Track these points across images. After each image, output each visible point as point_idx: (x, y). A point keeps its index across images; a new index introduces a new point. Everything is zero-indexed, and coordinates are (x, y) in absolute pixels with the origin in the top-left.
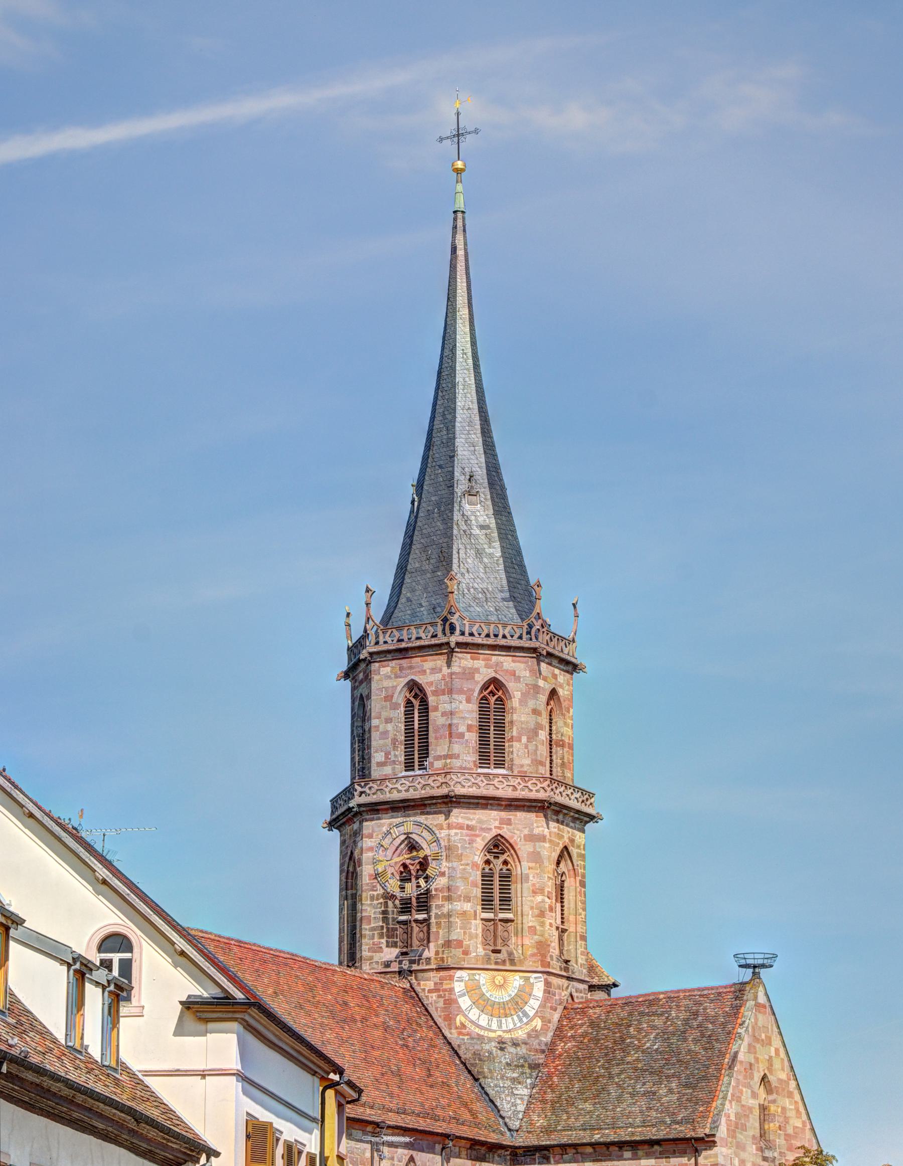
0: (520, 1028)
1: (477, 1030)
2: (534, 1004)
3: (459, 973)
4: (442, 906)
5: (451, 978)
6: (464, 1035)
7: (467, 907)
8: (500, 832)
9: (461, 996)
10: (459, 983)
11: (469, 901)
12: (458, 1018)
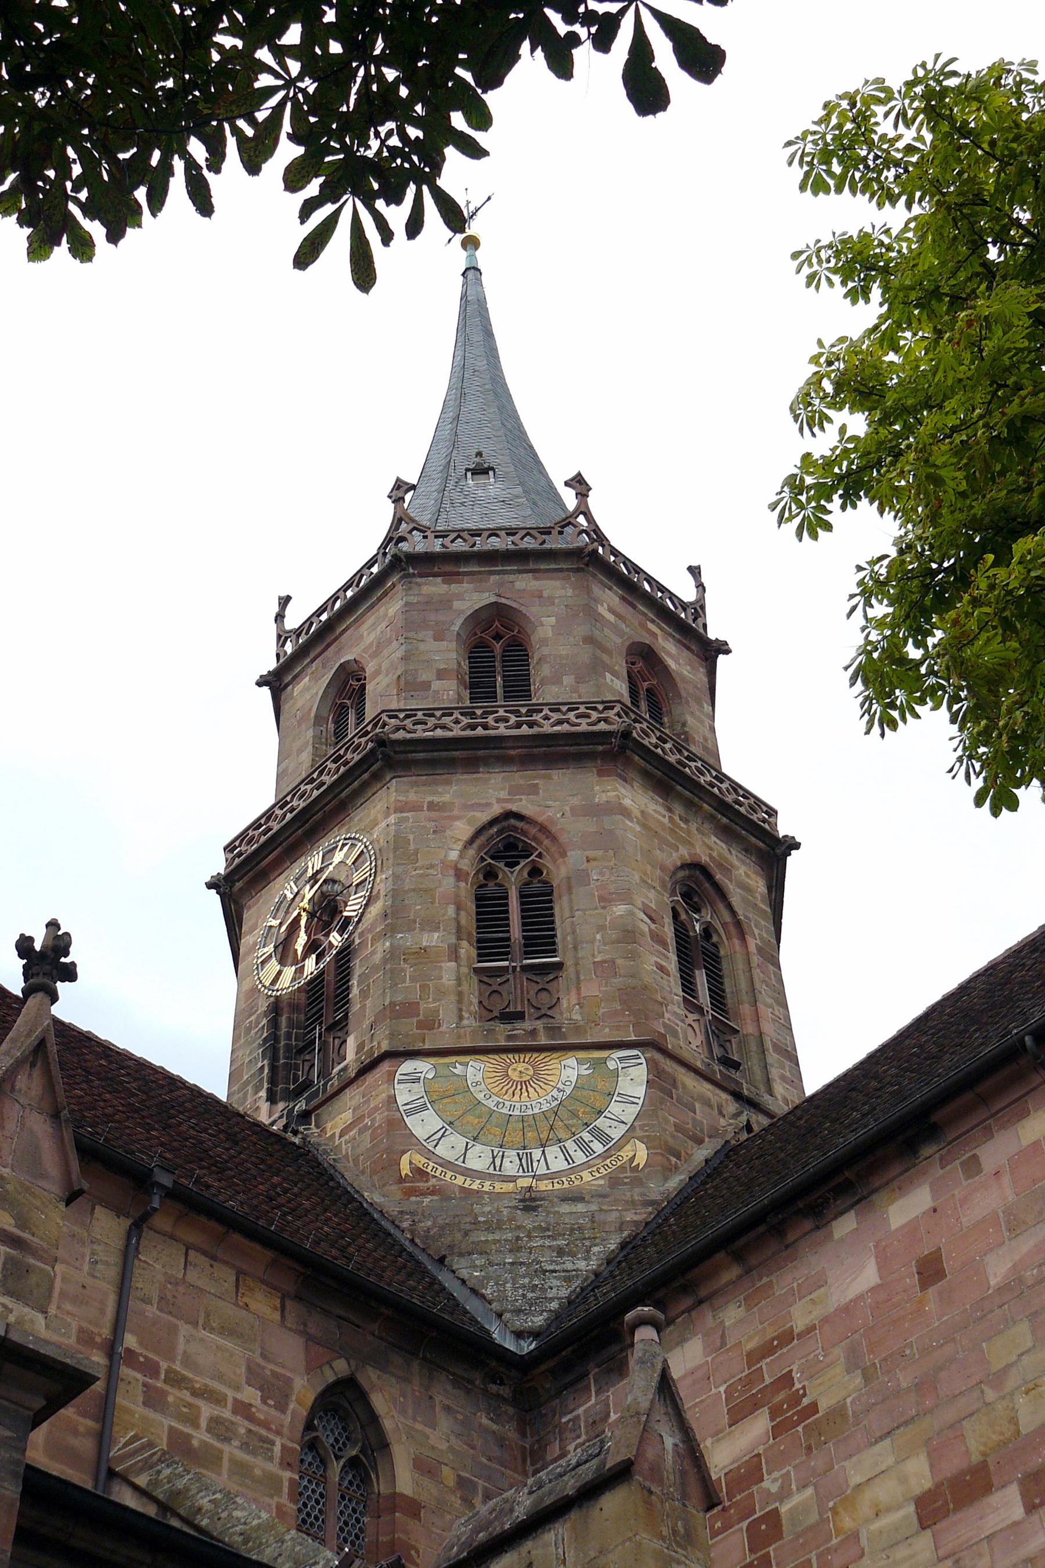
0: (586, 1165)
1: (460, 1180)
3: (408, 1067)
6: (423, 1194)
7: (432, 939)
8: (514, 808)
11: (437, 929)
12: (405, 1159)
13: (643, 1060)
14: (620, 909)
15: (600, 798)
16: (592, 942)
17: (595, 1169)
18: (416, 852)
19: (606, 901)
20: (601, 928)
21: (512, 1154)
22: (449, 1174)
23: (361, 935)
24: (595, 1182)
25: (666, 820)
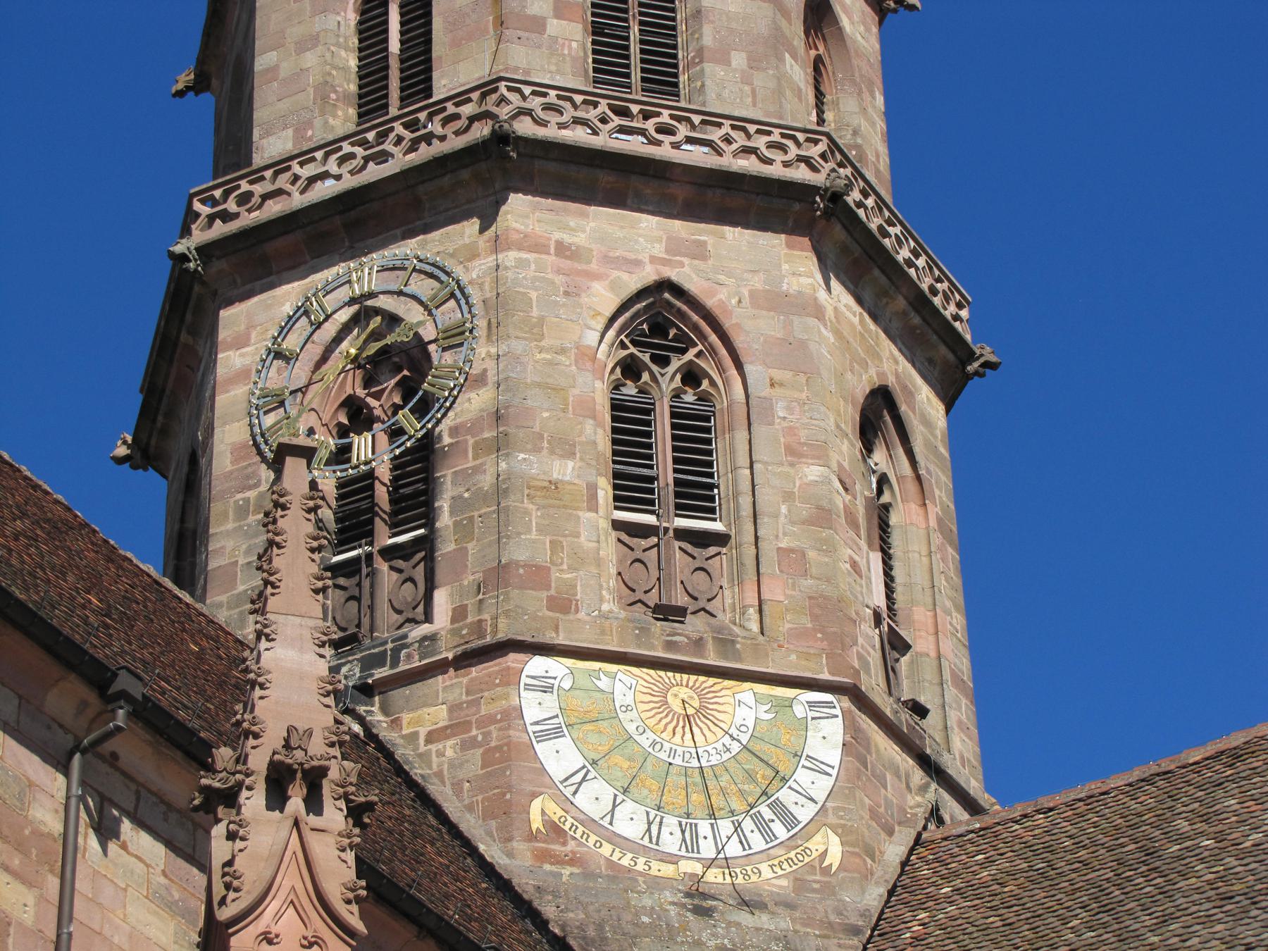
1: (606, 849)
2: (810, 787)
3: (538, 665)
4: (477, 470)
5: (511, 679)
6: (559, 861)
7: (565, 470)
8: (674, 275)
9: (544, 736)
10: (540, 690)
11: (572, 455)
12: (536, 806)
13: (838, 711)
14: (813, 472)
15: (792, 285)
16: (776, 516)
17: (776, 862)
18: (542, 320)
19: (795, 453)
20: (788, 496)
21: (671, 822)
22: (593, 838)
23: (454, 431)
24: (774, 881)
25: (856, 320)
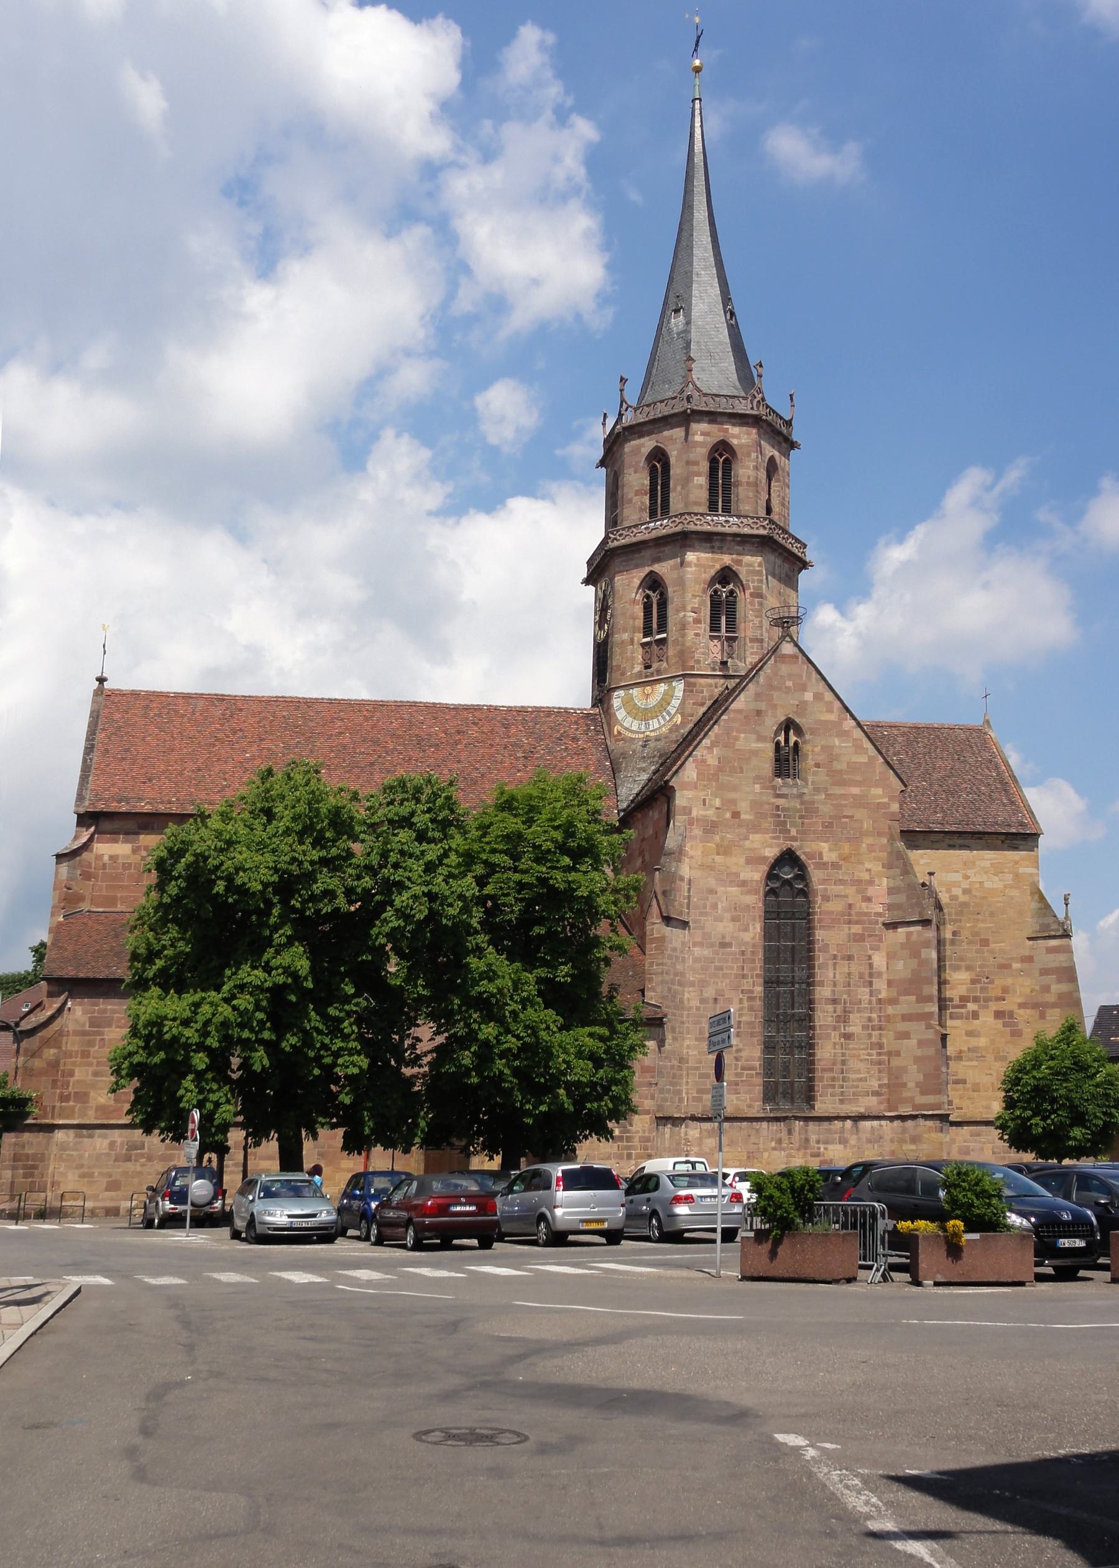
1: (630, 735)
2: (676, 703)
